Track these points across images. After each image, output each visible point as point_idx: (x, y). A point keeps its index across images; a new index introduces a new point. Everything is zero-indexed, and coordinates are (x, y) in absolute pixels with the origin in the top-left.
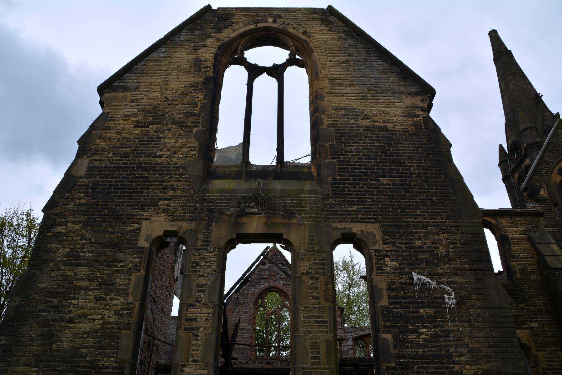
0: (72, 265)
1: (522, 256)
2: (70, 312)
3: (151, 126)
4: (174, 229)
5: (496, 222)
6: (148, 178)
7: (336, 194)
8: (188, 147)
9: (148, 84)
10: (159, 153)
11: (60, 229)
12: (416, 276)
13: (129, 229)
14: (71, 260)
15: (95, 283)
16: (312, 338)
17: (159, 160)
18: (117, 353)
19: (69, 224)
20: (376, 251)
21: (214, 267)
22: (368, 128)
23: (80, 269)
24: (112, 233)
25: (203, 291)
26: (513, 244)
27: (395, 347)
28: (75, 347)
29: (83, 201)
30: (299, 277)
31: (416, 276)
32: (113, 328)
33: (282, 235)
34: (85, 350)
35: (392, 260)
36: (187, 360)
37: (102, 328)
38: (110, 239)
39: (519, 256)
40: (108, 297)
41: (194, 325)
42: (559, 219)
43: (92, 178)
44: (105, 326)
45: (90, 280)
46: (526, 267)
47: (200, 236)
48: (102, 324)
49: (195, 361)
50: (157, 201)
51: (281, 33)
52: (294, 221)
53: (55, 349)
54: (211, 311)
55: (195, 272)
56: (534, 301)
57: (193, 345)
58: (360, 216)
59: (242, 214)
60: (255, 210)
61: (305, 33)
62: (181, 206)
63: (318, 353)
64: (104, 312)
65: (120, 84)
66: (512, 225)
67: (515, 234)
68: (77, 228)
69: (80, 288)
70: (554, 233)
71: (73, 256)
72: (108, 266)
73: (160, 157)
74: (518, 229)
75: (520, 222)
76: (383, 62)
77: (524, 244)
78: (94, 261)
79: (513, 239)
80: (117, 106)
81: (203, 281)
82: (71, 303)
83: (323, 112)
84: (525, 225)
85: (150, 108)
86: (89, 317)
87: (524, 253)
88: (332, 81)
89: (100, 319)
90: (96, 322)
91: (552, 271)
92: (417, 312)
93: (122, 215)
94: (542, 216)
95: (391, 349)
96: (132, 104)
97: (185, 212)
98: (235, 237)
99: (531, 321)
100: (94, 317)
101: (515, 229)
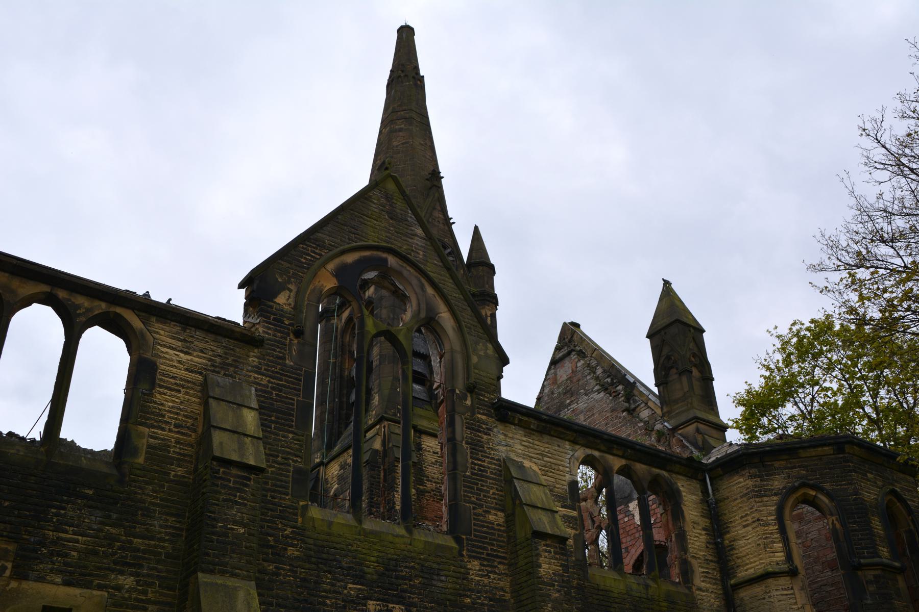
1: (170, 417)
5: (142, 326)
26: (161, 386)
39: (163, 416)
42: (292, 363)
46: (169, 446)
56: (151, 525)
66: (179, 344)
67: (176, 367)
70: (269, 389)
74: (189, 357)
75: (202, 345)
77: (187, 393)
79: (167, 376)
84: (211, 353)
87: (177, 414)
91: (215, 463)
94: (257, 347)
99: (121, 573)
101: (182, 355)
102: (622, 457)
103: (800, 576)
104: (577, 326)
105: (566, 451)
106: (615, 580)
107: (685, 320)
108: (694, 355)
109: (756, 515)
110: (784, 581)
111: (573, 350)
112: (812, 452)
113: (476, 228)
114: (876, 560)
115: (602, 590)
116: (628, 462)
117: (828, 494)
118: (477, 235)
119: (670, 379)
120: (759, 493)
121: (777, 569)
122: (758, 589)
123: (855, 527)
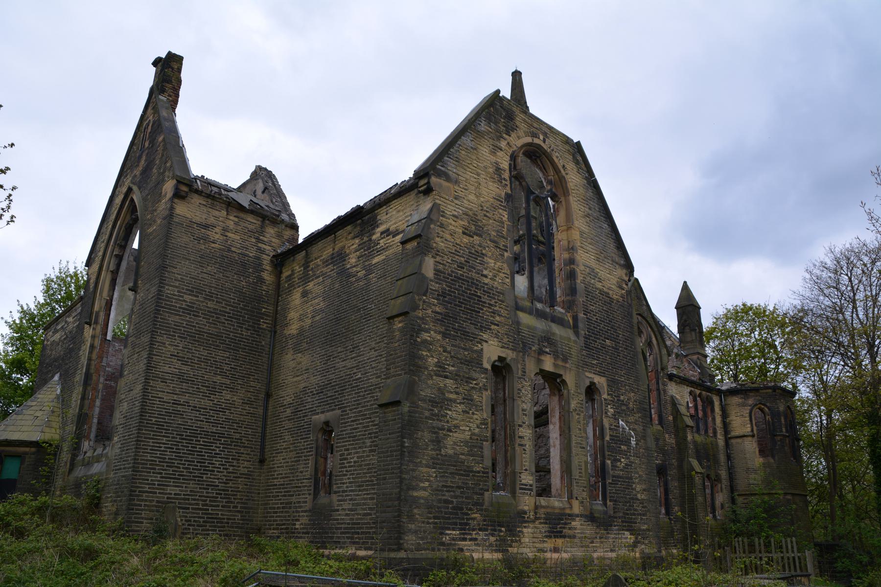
0: (441, 376)
2: (448, 422)
3: (475, 237)
4: (503, 355)
6: (480, 297)
7: (587, 348)
8: (504, 273)
9: (465, 179)
10: (485, 272)
11: (425, 336)
12: (621, 422)
13: (476, 348)
14: (439, 371)
15: (460, 397)
16: (579, 459)
17: (486, 281)
18: (483, 460)
19: (432, 332)
20: (605, 399)
21: (530, 395)
22: (601, 292)
23: (448, 381)
24: (465, 349)
25: (526, 415)
27: (612, 470)
28: (456, 454)
29: (437, 309)
30: (572, 412)
31: (621, 422)
32: (477, 439)
33: (562, 375)
34: (463, 457)
35: (611, 408)
36: (522, 469)
37: (471, 438)
38: (465, 355)
40: (471, 411)
41: (523, 442)
43: (440, 284)
44: (473, 437)
45: (457, 393)
47: (520, 366)
48: (471, 435)
49: (526, 470)
50: (490, 324)
51: (547, 157)
52: (567, 365)
53: (444, 454)
54: (531, 431)
55: (520, 397)
57: (524, 457)
58: (597, 369)
59: (541, 352)
60: (547, 350)
61: (564, 166)
62: (506, 334)
63: (581, 469)
64: (471, 425)
65: (443, 169)
68: (438, 338)
69: (450, 400)
71: (440, 367)
72: (467, 382)
73: (486, 276)
76: (608, 225)
78: (456, 375)
80: (445, 198)
81: (525, 407)
82: (447, 414)
83: (578, 265)
85: (470, 213)
86: (461, 428)
88: (582, 233)
89: (469, 431)
90: (467, 433)
92: (620, 448)
93: (469, 333)
95: (610, 471)
96: (456, 202)
97: (508, 341)
98: (538, 371)
100: (463, 428)
107: (694, 304)
108: (697, 321)
109: (742, 413)
110: (750, 438)
112: (765, 391)
114: (782, 433)
120: (744, 405)
121: (748, 434)
122: (739, 440)
123: (776, 421)
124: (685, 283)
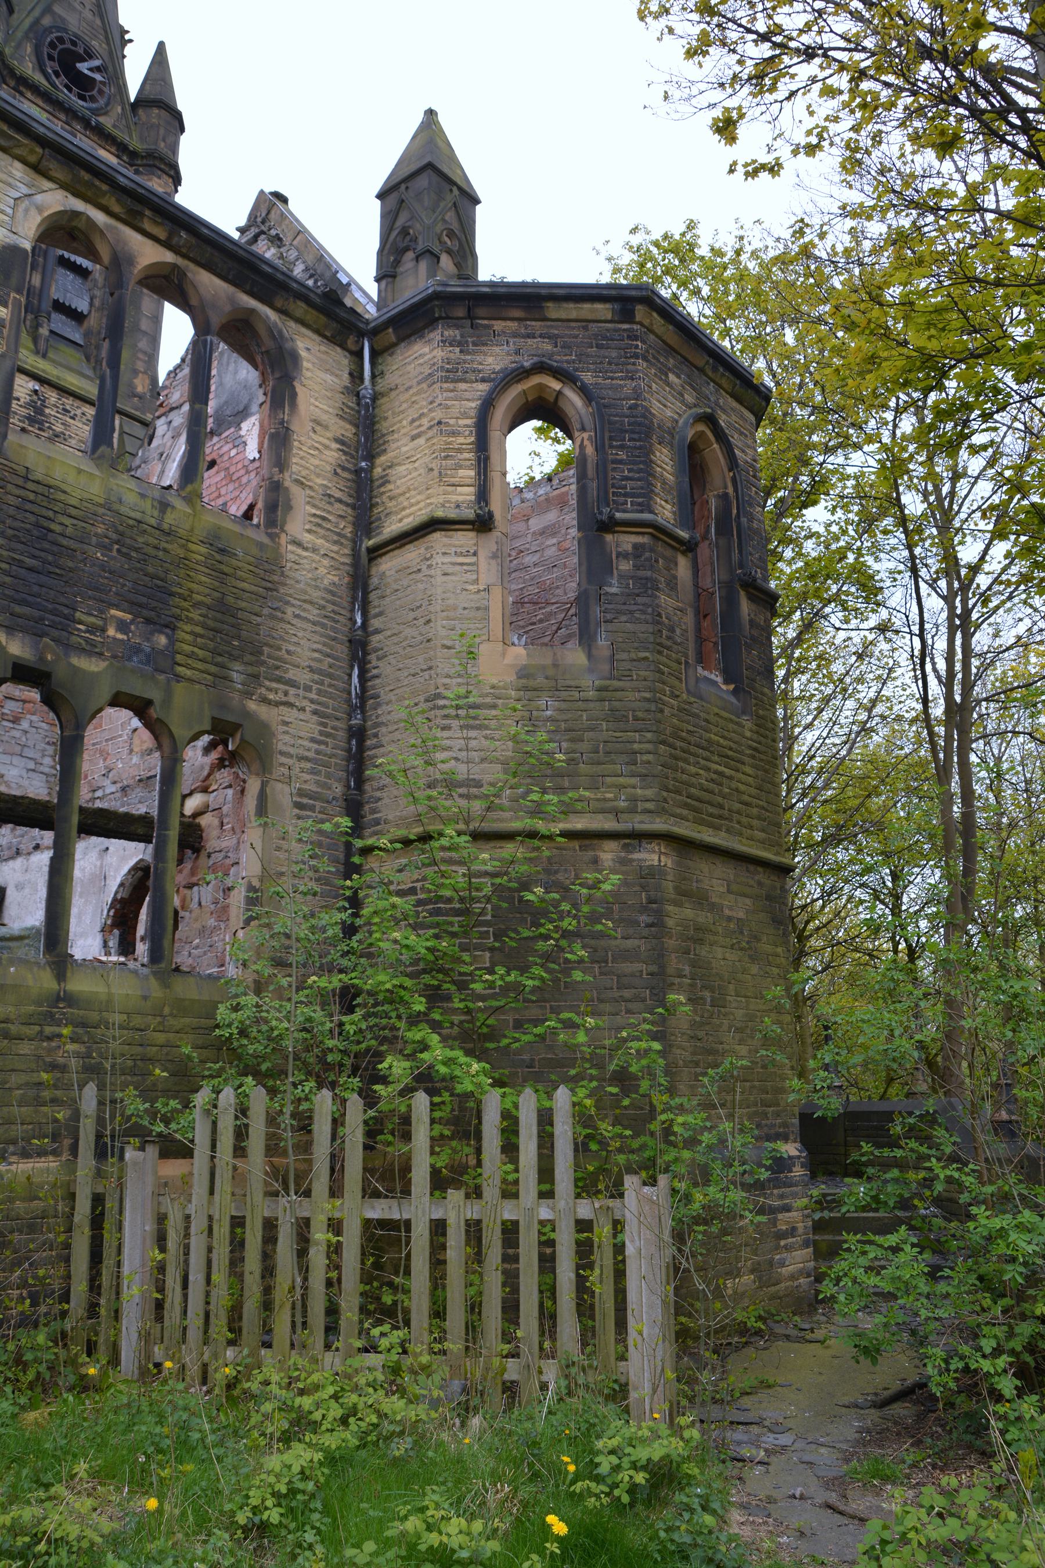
102: (167, 245)
103: (496, 534)
104: (284, 200)
105: (11, 180)
106: (80, 471)
107: (446, 170)
108: (451, 234)
109: (438, 415)
110: (464, 539)
111: (263, 232)
112: (571, 311)
113: (161, 46)
114: (646, 516)
115: (38, 482)
116: (180, 261)
117: (584, 391)
118: (160, 57)
119: (401, 269)
120: (452, 374)
121: (452, 514)
122: (411, 555)
123: (622, 455)
124: (431, 114)
